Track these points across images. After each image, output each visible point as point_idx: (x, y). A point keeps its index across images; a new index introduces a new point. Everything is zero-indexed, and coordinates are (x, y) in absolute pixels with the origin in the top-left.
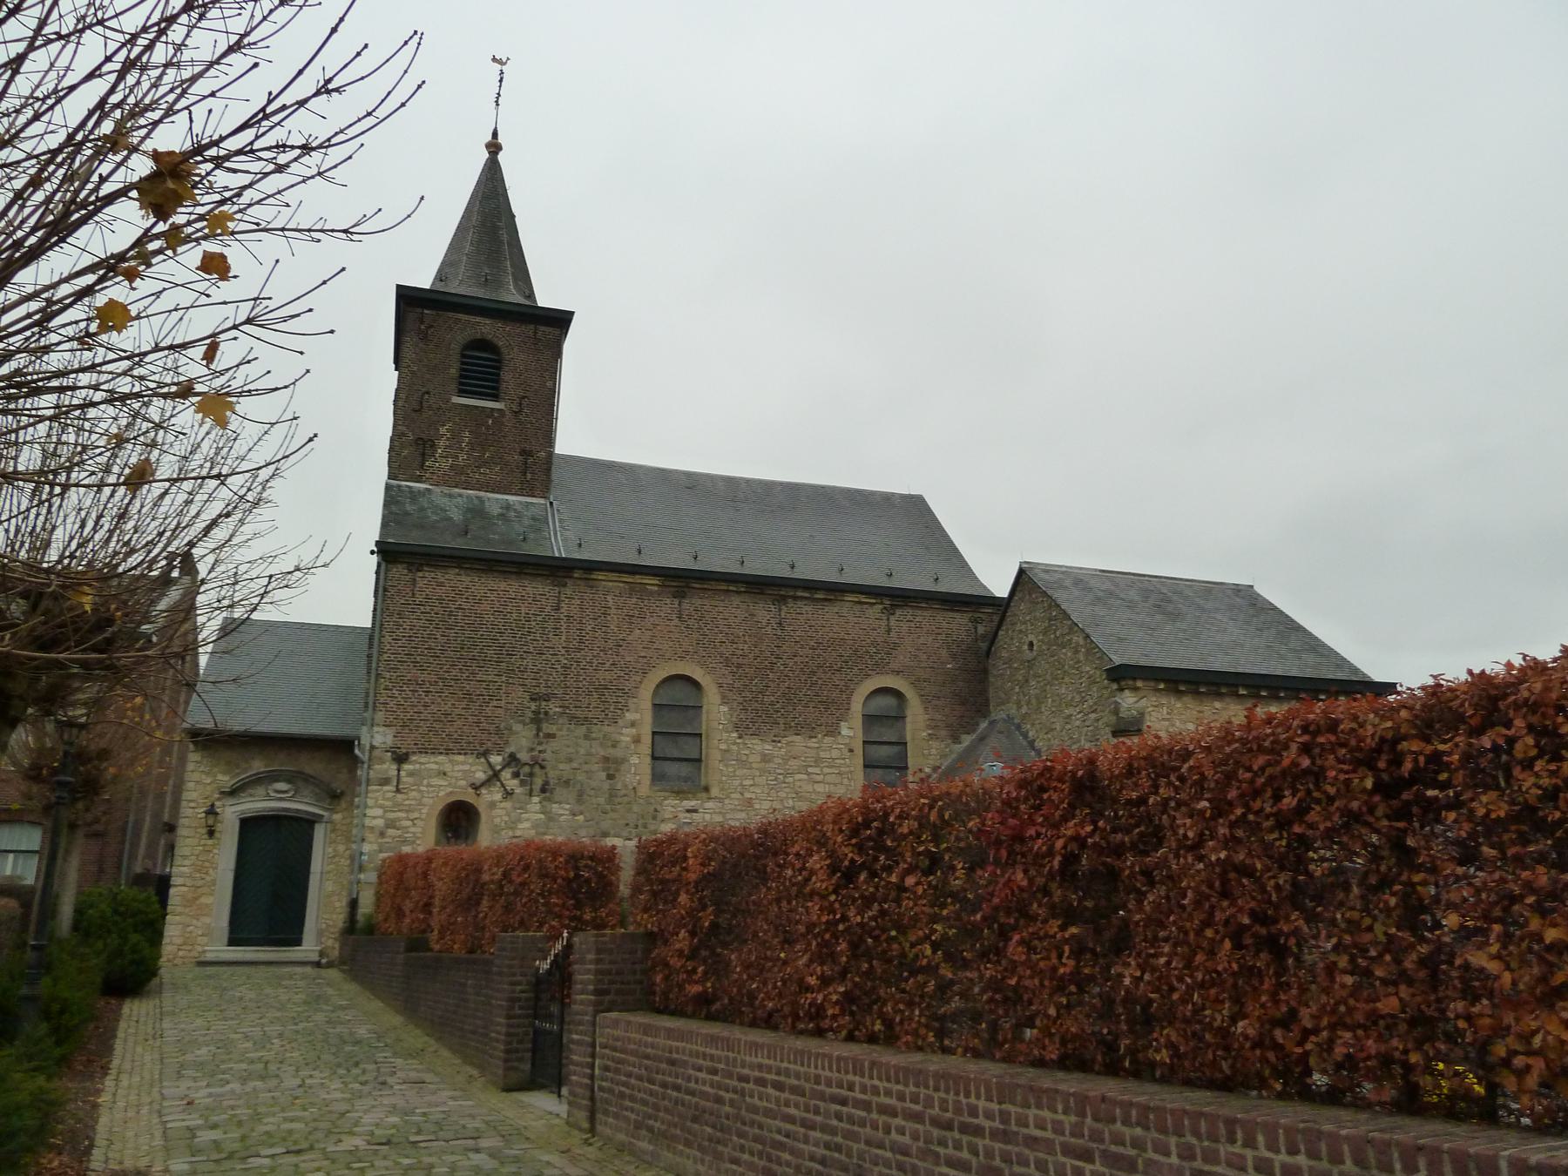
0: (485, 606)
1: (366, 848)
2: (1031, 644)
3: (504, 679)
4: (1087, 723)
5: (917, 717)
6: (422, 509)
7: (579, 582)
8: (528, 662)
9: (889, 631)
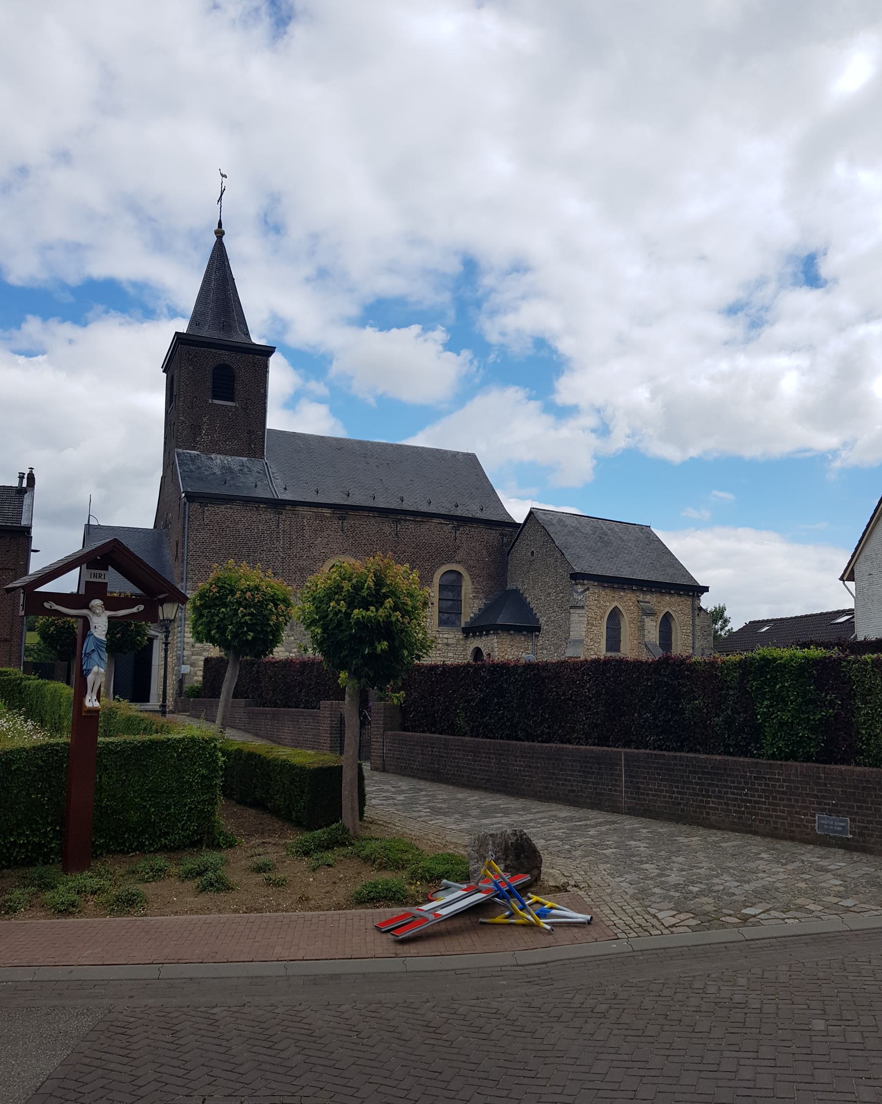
0: (240, 526)
1: (186, 653)
2: (533, 552)
3: (252, 565)
4: (558, 598)
5: (467, 587)
6: (199, 468)
7: (289, 512)
8: (264, 556)
9: (455, 540)
